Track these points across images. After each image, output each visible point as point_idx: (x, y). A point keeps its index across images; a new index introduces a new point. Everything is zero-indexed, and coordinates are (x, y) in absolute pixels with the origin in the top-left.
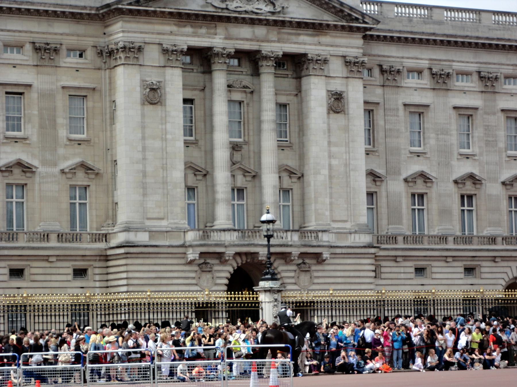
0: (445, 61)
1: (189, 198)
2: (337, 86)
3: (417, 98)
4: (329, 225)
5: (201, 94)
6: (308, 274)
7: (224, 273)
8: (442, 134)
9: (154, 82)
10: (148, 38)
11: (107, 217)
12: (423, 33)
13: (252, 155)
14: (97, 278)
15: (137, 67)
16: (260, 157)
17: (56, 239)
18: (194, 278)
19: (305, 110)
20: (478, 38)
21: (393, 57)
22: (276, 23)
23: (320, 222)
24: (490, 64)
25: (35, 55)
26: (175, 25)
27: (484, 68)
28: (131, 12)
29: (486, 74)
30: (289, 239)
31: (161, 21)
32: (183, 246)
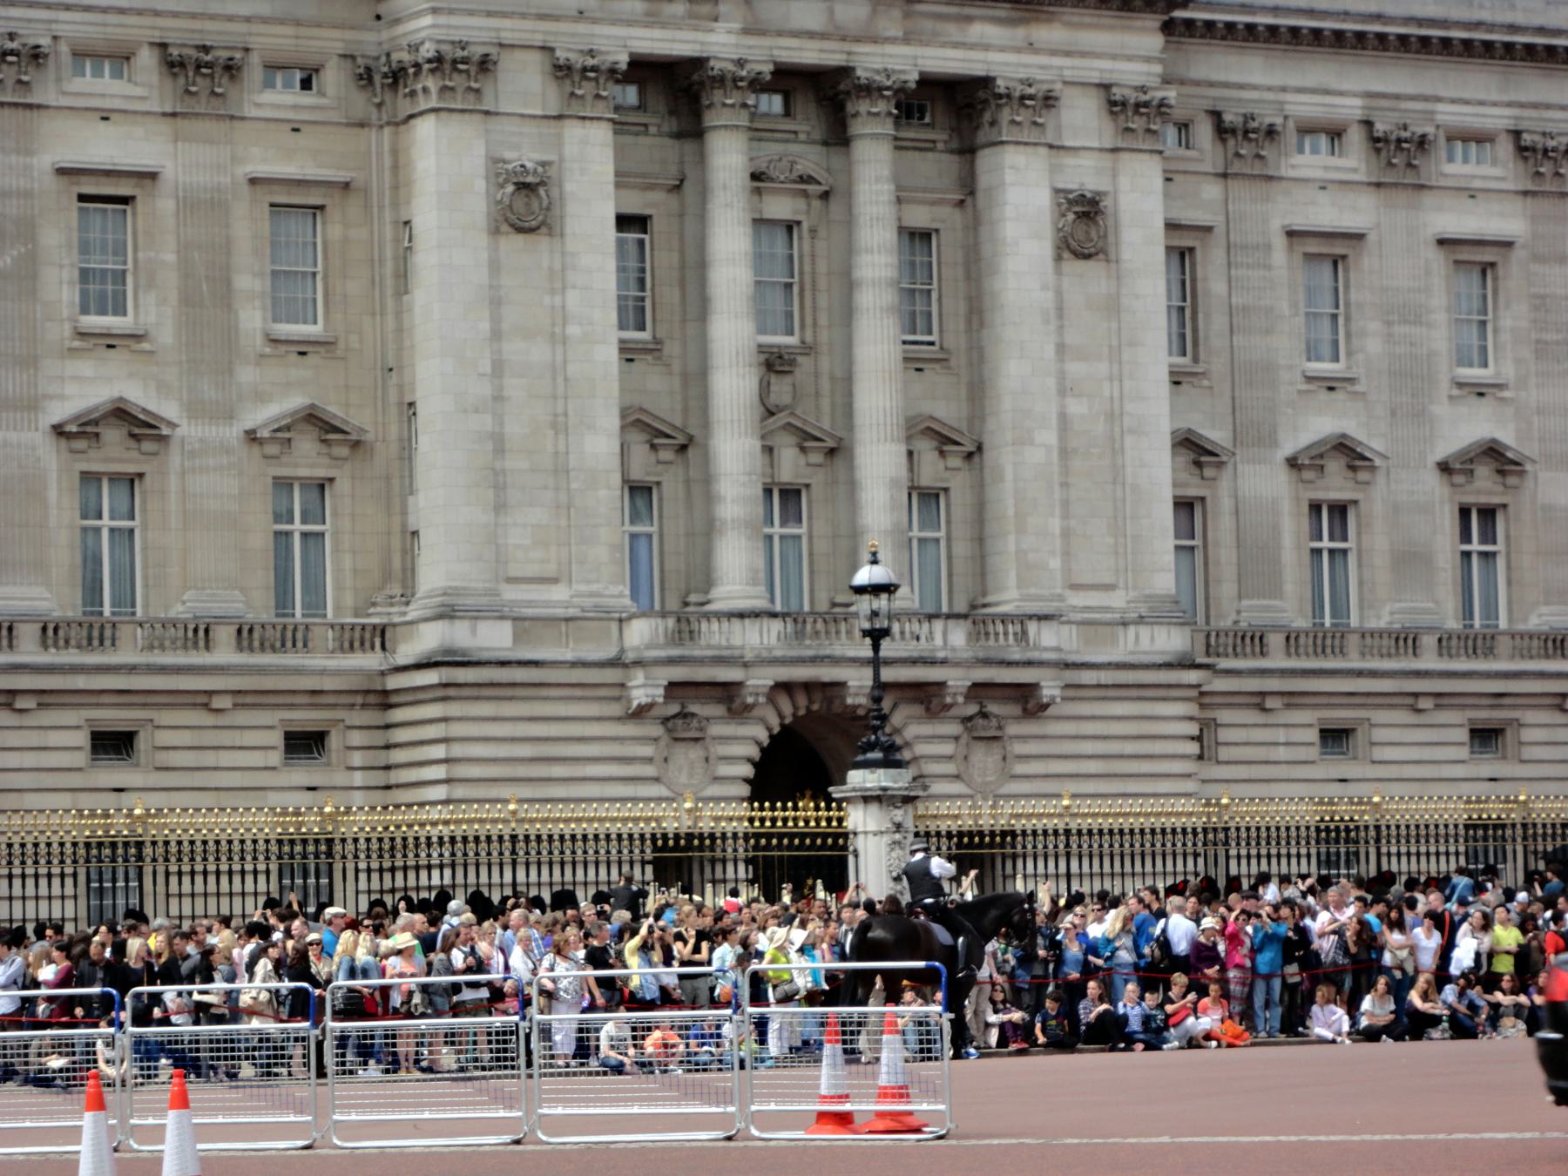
1: (635, 518)
2: (1084, 175)
3: (1327, 214)
4: (1061, 598)
5: (673, 200)
6: (996, 748)
7: (739, 744)
8: (1405, 321)
9: (529, 165)
10: (511, 30)
11: (387, 577)
12: (1346, 13)
13: (825, 385)
14: (357, 759)
16: (849, 394)
17: (233, 641)
18: (650, 760)
19: (986, 250)
20: (1513, 28)
21: (1255, 87)
23: (1032, 591)
24: (1548, 107)
25: (168, 82)
27: (1532, 121)
29: (1537, 138)
30: (939, 641)
32: (615, 663)
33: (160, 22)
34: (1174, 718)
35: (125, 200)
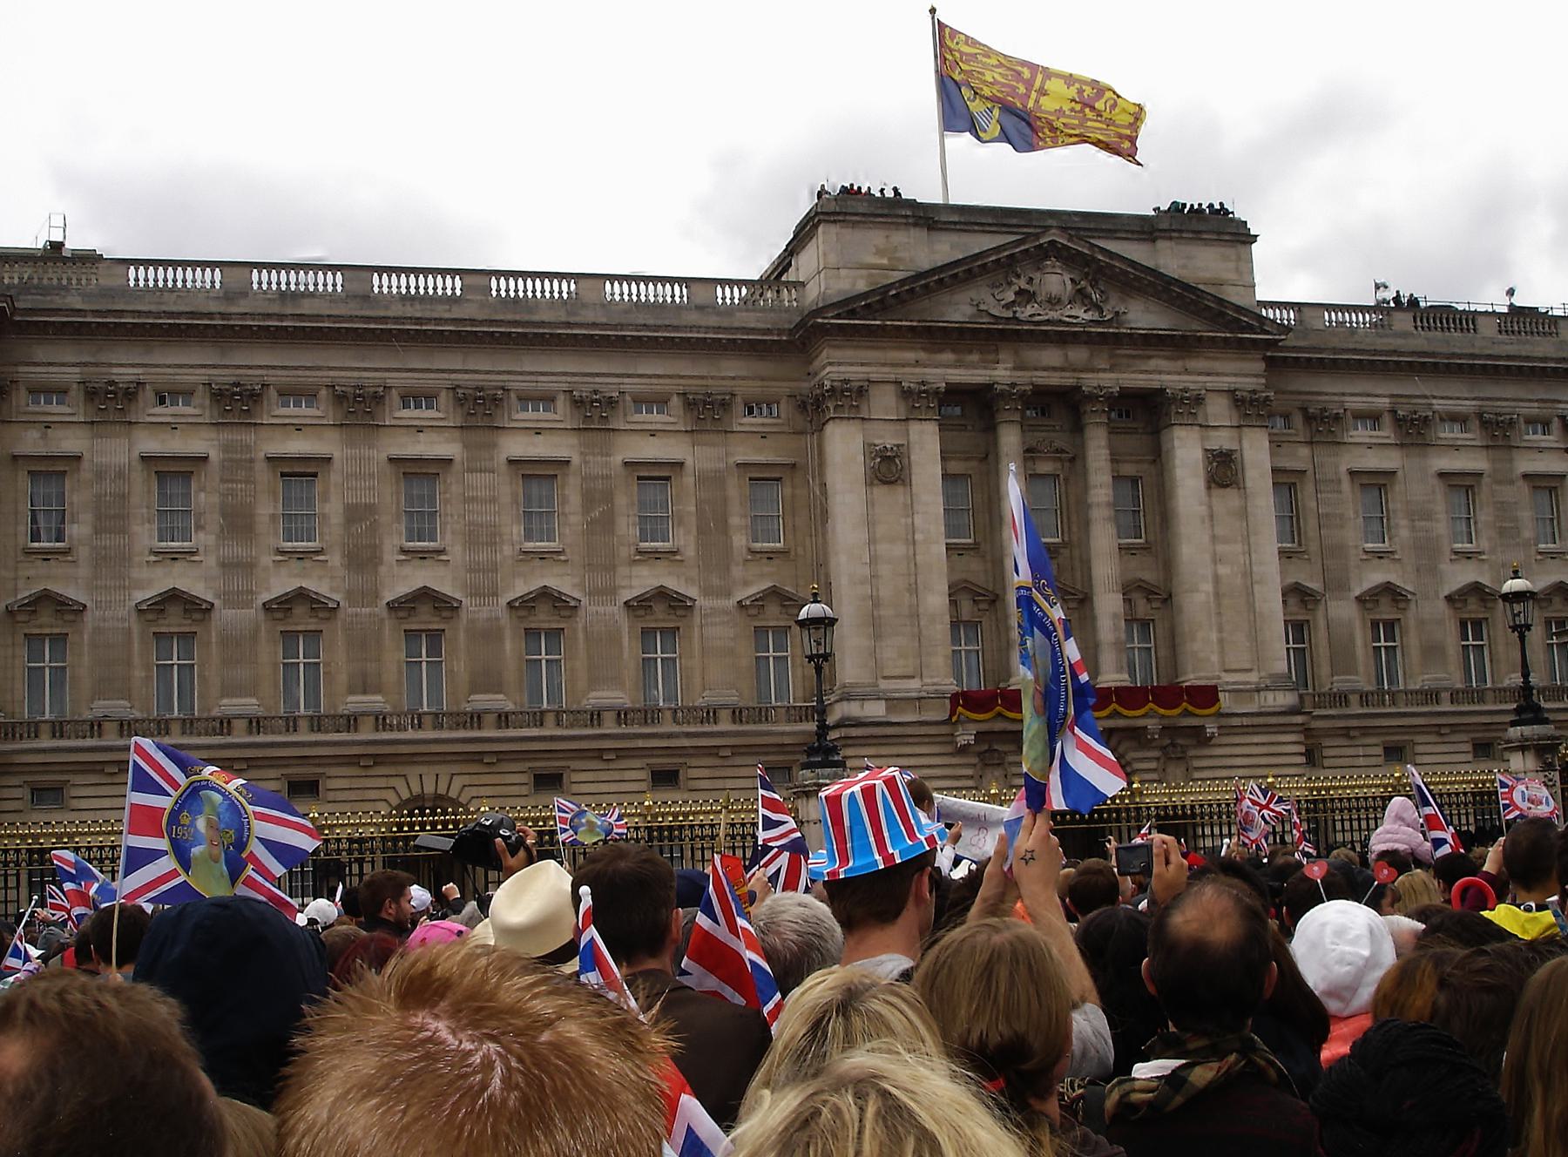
2: (1222, 440)
10: (875, 373)
16: (1090, 569)
26: (923, 349)
34: (1291, 745)
35: (668, 479)
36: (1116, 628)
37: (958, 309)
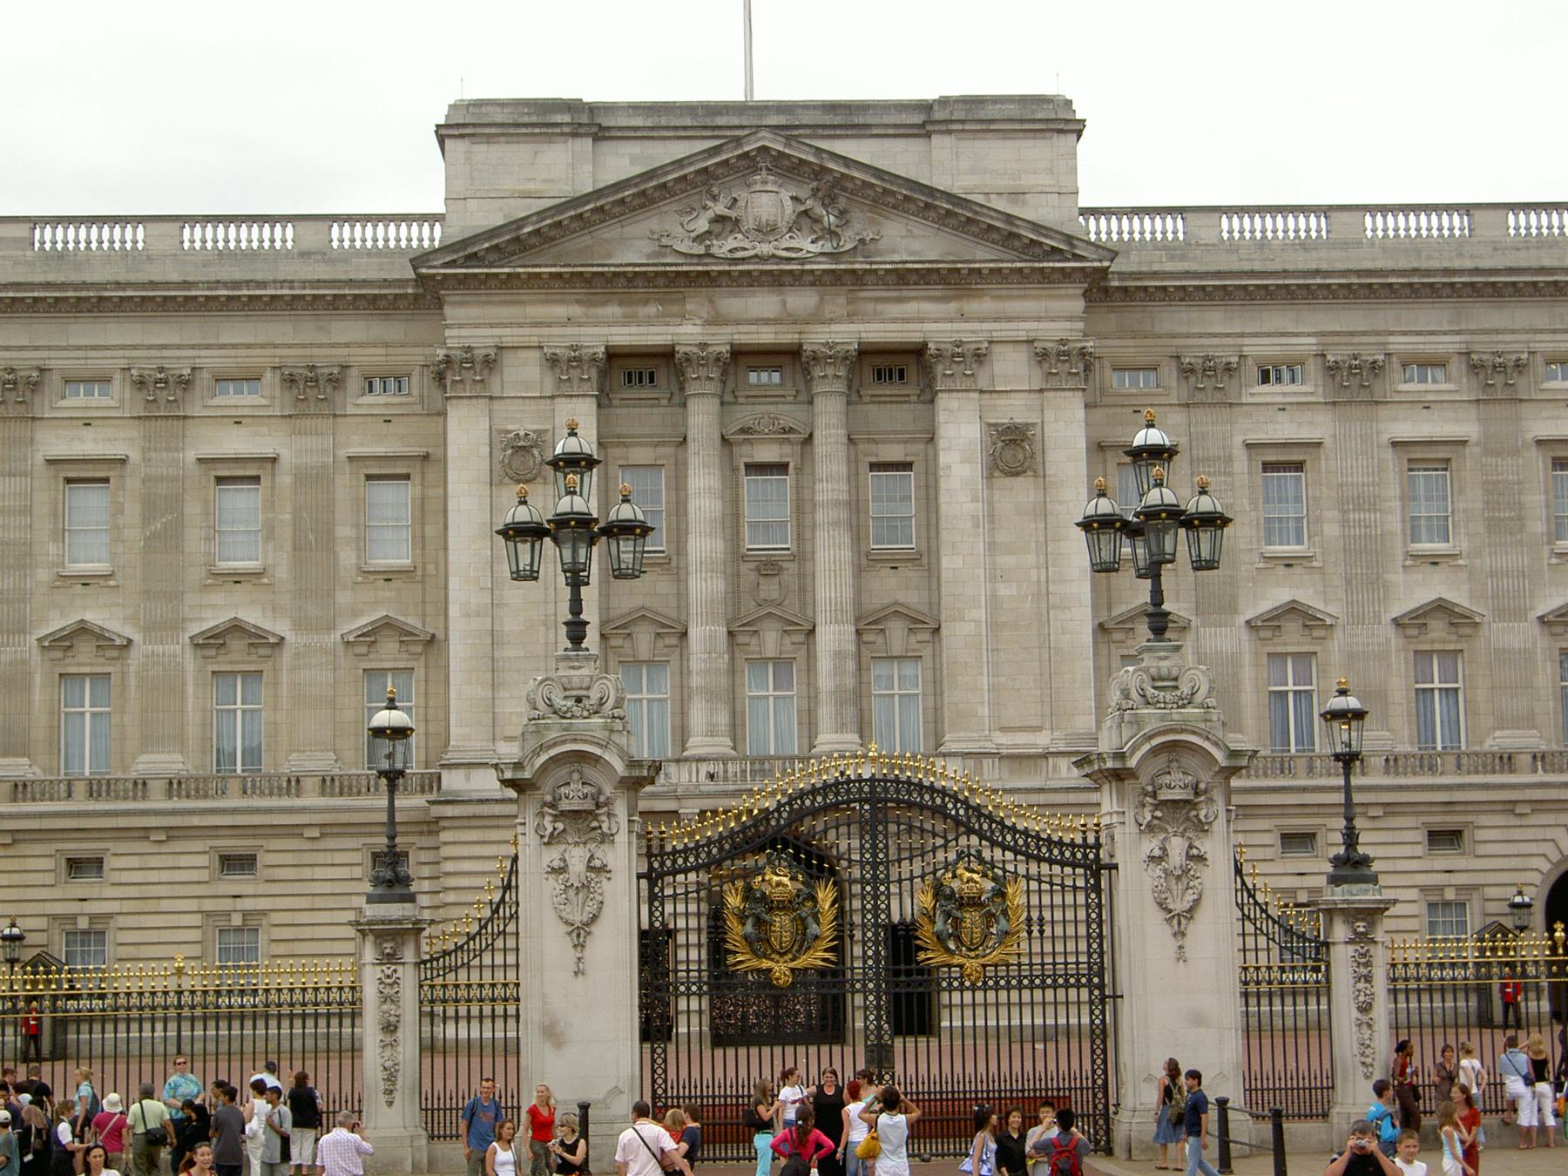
0: (1364, 333)
2: (1015, 410)
3: (1286, 429)
9: (522, 433)
10: (509, 336)
15: (482, 401)
22: (836, 278)
24: (1498, 332)
26: (578, 302)
27: (1483, 347)
28: (463, 281)
31: (542, 297)
33: (279, 352)
36: (838, 671)
37: (630, 246)
